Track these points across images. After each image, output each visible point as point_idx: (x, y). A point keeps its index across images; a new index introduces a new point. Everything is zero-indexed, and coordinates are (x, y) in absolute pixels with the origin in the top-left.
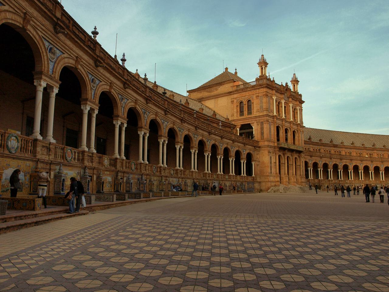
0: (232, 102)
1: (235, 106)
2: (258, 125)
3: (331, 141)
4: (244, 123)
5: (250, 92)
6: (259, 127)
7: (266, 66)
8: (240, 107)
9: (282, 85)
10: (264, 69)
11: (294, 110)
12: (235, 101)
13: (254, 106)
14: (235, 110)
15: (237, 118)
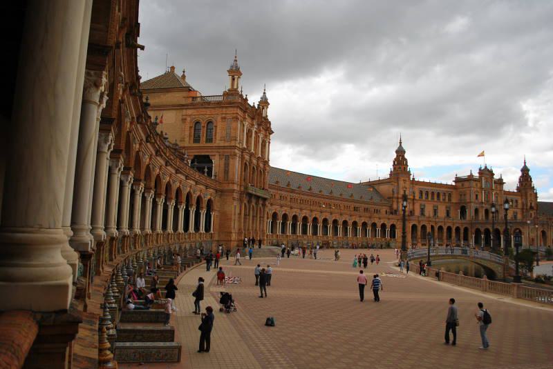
0: (184, 120)
1: (188, 126)
2: (220, 159)
3: (288, 185)
4: (199, 154)
5: (213, 110)
6: (223, 162)
7: (239, 77)
8: (195, 130)
9: (254, 106)
10: (236, 80)
11: (264, 142)
12: (189, 119)
13: (218, 131)
14: (187, 133)
15: (190, 145)
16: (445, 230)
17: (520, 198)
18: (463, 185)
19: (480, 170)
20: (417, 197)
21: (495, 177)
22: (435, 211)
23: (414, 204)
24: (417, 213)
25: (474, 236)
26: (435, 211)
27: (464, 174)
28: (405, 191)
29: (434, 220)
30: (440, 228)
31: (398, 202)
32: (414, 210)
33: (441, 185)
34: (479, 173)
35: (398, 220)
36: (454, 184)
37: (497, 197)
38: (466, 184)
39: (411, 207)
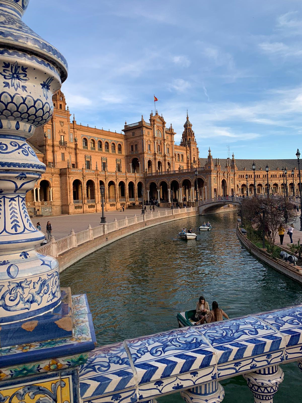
17: (185, 152)
18: (134, 134)
19: (151, 115)
21: (166, 125)
22: (104, 165)
23: (76, 154)
25: (148, 191)
26: (104, 165)
27: (133, 121)
29: (103, 173)
32: (77, 163)
33: (109, 134)
34: (150, 120)
35: (52, 174)
36: (123, 133)
38: (137, 132)
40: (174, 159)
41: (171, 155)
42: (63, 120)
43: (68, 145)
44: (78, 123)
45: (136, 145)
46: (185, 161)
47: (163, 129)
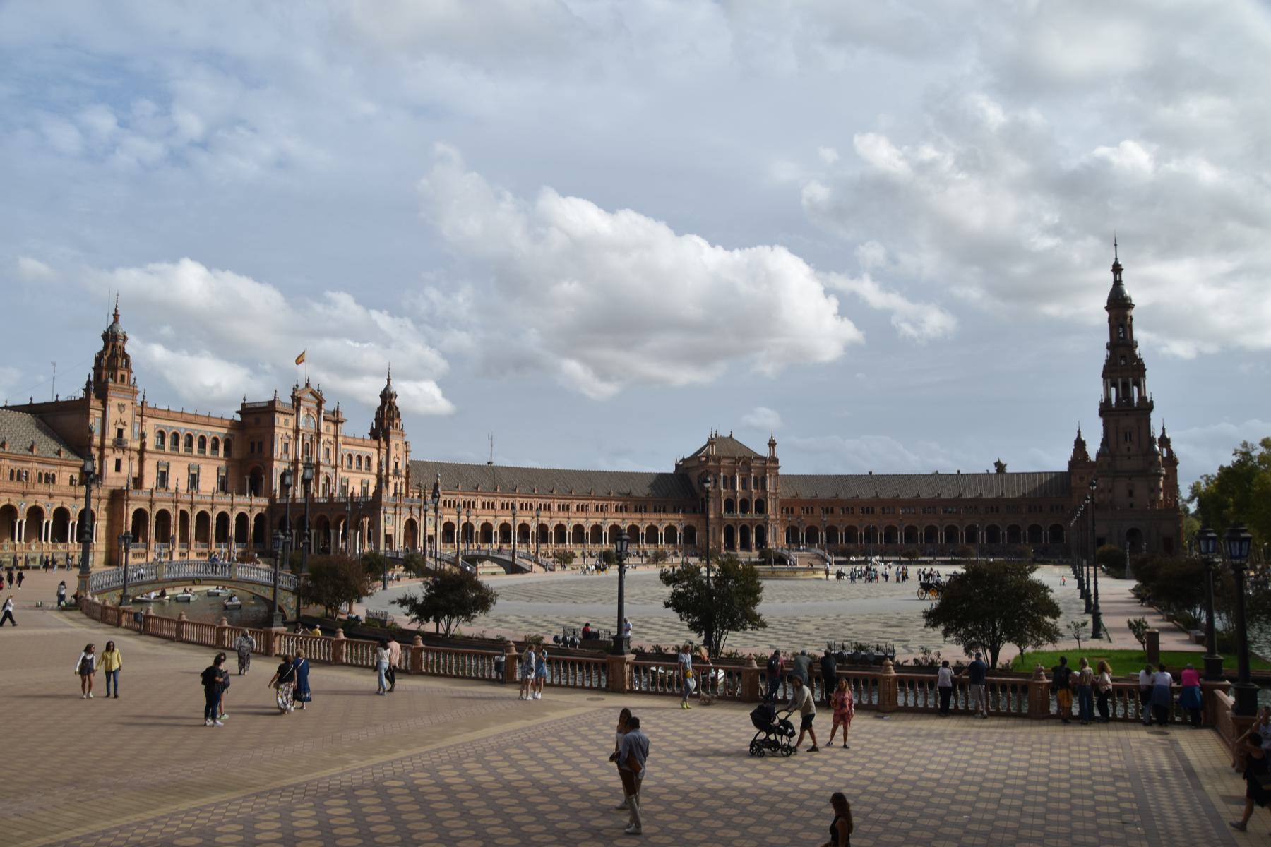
16: (214, 522)
17: (375, 451)
18: (257, 421)
19: (295, 390)
20: (151, 442)
22: (194, 480)
23: (141, 462)
24: (150, 480)
26: (194, 480)
28: (120, 432)
30: (203, 517)
31: (102, 458)
34: (293, 397)
36: (238, 418)
37: (328, 450)
39: (136, 469)
40: (339, 470)
41: (332, 462)
42: (124, 402)
43: (128, 445)
44: (151, 405)
45: (261, 445)
46: (375, 469)
47: (319, 413)
